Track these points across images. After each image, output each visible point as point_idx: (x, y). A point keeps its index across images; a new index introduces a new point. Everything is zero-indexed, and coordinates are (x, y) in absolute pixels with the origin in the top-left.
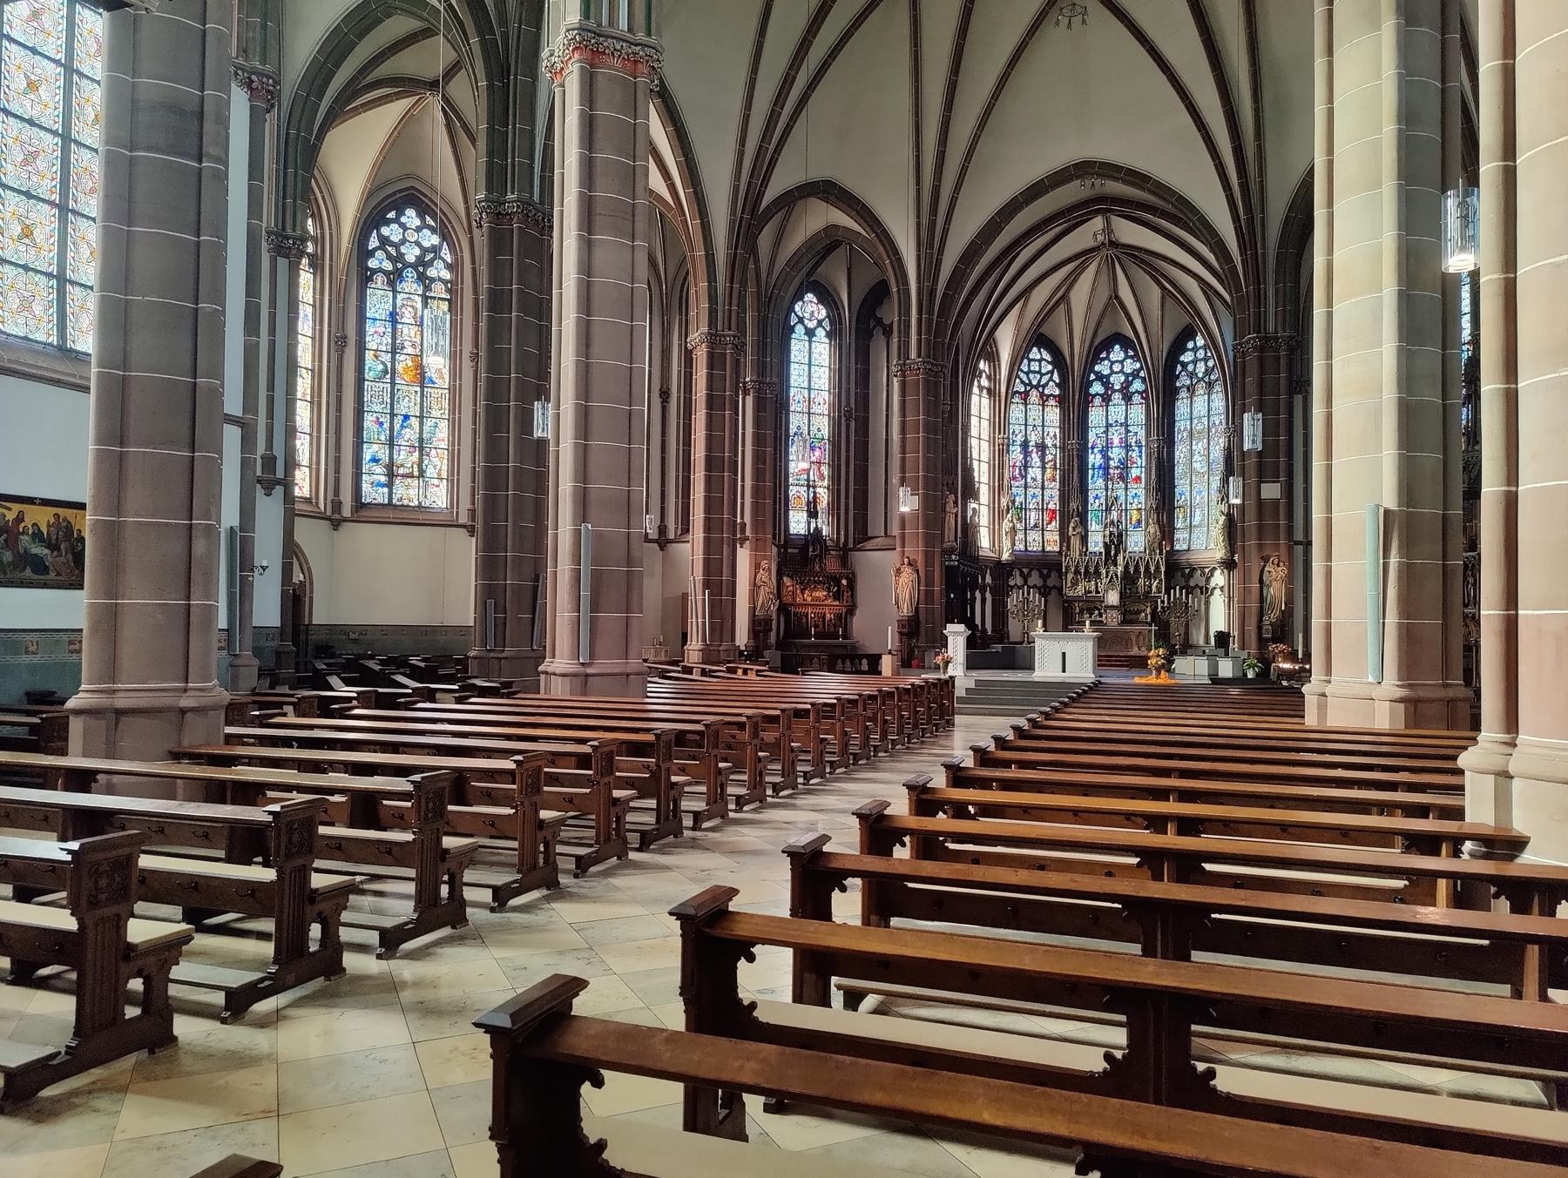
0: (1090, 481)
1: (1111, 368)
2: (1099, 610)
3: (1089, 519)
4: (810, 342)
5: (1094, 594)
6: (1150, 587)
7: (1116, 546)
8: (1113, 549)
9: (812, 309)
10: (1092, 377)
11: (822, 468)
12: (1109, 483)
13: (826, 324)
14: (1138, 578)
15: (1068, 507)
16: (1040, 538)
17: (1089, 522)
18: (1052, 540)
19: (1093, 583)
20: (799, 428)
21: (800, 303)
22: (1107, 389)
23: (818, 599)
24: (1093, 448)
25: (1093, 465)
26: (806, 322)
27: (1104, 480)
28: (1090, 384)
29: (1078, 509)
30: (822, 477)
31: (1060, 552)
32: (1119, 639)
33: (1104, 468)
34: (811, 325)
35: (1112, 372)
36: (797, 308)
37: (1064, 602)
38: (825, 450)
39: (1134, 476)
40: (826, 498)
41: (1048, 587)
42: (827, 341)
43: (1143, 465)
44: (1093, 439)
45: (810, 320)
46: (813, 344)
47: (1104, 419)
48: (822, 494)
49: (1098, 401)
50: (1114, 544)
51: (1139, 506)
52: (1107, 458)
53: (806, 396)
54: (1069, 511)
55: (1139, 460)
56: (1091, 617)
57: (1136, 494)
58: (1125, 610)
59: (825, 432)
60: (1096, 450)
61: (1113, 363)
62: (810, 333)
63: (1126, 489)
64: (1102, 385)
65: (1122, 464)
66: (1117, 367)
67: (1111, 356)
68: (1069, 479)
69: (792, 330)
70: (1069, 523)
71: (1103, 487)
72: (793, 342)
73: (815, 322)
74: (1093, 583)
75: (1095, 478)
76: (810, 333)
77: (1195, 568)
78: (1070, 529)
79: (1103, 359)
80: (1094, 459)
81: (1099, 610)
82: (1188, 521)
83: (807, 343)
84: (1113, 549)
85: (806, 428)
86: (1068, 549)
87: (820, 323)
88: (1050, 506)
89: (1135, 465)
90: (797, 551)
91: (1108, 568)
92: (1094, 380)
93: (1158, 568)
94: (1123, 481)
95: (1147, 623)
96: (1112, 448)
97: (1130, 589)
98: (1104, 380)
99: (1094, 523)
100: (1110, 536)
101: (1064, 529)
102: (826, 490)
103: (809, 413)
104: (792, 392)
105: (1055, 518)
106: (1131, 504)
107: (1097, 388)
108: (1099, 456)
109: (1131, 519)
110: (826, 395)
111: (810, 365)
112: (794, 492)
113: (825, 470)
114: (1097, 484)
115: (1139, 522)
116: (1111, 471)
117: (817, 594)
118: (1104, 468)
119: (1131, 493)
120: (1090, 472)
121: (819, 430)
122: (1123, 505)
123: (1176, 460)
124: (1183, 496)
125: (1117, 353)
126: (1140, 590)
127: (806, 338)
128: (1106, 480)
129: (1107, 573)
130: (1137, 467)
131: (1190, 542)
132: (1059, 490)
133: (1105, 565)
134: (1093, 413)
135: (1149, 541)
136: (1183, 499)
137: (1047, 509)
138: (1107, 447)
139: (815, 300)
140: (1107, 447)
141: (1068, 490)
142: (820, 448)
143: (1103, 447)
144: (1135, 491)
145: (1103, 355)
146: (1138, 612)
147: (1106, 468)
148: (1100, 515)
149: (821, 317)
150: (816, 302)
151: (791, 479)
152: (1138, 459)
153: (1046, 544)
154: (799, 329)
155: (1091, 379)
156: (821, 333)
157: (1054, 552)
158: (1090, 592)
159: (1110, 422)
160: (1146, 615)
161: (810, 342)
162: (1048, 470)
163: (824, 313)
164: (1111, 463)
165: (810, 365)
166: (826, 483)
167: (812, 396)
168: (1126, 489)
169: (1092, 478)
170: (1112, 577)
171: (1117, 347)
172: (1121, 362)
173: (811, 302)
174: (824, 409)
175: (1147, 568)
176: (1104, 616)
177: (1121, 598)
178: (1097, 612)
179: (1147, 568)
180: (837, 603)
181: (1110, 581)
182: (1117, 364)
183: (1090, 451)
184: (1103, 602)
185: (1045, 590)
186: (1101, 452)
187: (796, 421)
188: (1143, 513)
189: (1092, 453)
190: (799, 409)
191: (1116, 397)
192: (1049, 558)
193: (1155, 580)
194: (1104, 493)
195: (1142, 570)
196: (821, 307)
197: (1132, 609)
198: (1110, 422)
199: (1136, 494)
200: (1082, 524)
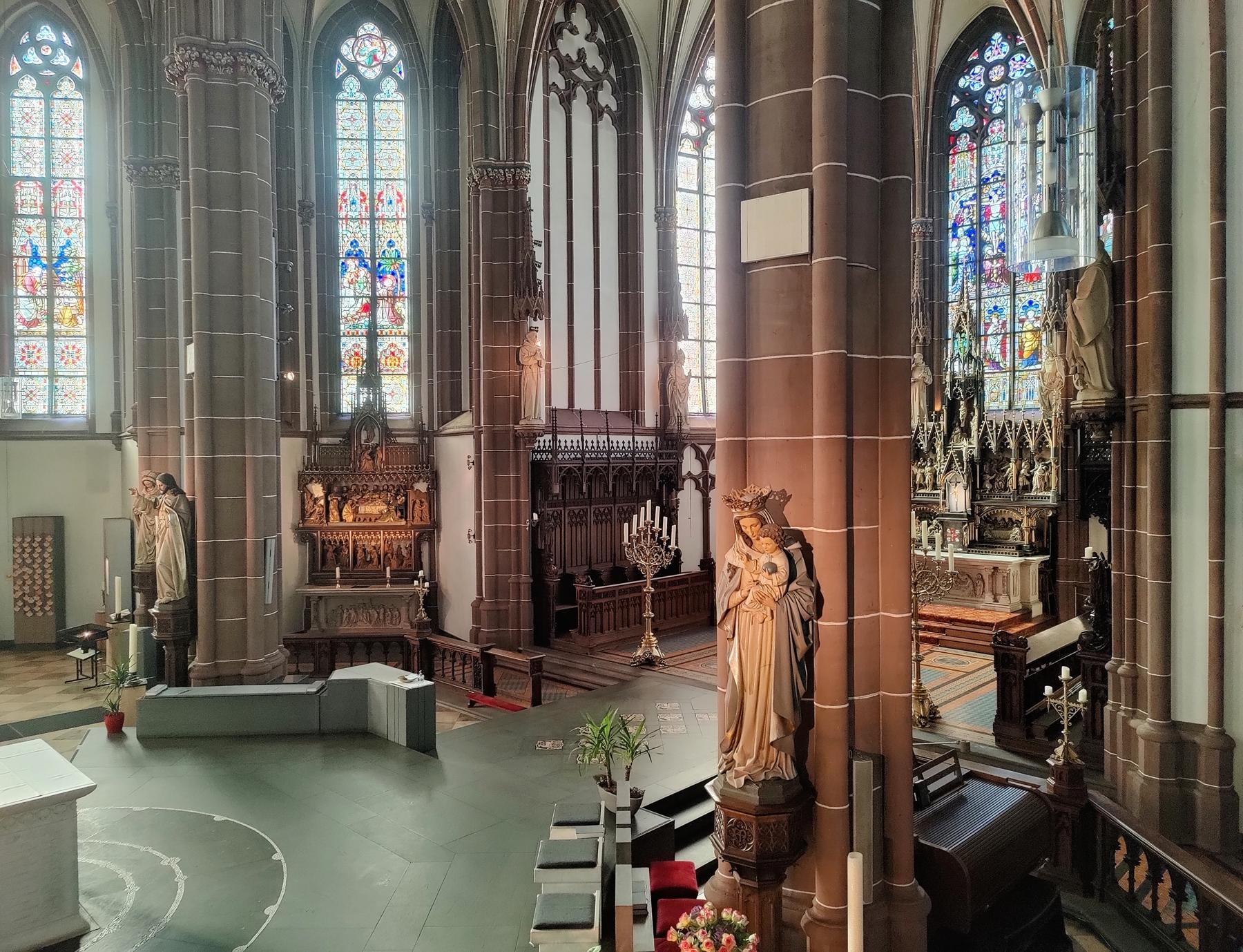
1: (986, 76)
4: (370, 102)
6: (1030, 478)
9: (372, 48)
10: (955, 100)
11: (398, 304)
13: (400, 69)
20: (354, 243)
21: (351, 41)
22: (980, 118)
23: (368, 518)
24: (955, 226)
25: (957, 259)
26: (361, 69)
28: (951, 114)
30: (397, 319)
33: (974, 262)
34: (370, 74)
35: (989, 84)
36: (345, 50)
38: (402, 276)
40: (406, 353)
42: (400, 97)
44: (955, 214)
45: (370, 67)
46: (376, 106)
47: (974, 173)
48: (400, 346)
49: (963, 142)
52: (978, 242)
53: (367, 192)
59: (403, 247)
60: (960, 232)
61: (989, 67)
62: (370, 89)
63: (1014, 294)
64: (971, 112)
66: (997, 74)
67: (987, 54)
69: (337, 86)
72: (339, 107)
73: (378, 70)
76: (370, 89)
79: (974, 64)
80: (959, 247)
83: (364, 106)
85: (368, 244)
87: (388, 70)
90: (337, 440)
92: (957, 106)
93: (1042, 443)
94: (1008, 282)
96: (987, 222)
98: (973, 101)
102: (406, 340)
103: (373, 219)
104: (342, 187)
106: (1022, 321)
107: (964, 119)
108: (965, 241)
109: (1021, 351)
110: (402, 187)
111: (371, 140)
112: (349, 346)
113: (404, 308)
115: (1036, 353)
116: (987, 265)
117: (364, 509)
118: (974, 262)
119: (1023, 299)
120: (952, 271)
121: (391, 244)
122: (1008, 326)
125: (998, 47)
127: (362, 96)
128: (978, 283)
134: (955, 165)
138: (980, 223)
139: (377, 32)
140: (980, 223)
142: (393, 274)
143: (972, 224)
145: (973, 57)
146: (1010, 524)
147: (977, 261)
149: (389, 59)
150: (379, 35)
151: (342, 327)
154: (351, 84)
155: (953, 104)
156: (389, 85)
158: (922, 486)
159: (985, 174)
161: (370, 102)
163: (393, 51)
164: (988, 251)
165: (371, 140)
166: (406, 328)
167: (377, 191)
168: (1014, 294)
169: (954, 281)
171: (997, 36)
172: (1005, 62)
173: (370, 36)
174: (401, 210)
175: (1022, 443)
179: (1022, 443)
180: (403, 523)
182: (996, 69)
183: (950, 235)
186: (969, 233)
187: (350, 233)
189: (954, 236)
190: (354, 215)
191: (996, 129)
195: (1012, 445)
196: (388, 43)
198: (985, 174)
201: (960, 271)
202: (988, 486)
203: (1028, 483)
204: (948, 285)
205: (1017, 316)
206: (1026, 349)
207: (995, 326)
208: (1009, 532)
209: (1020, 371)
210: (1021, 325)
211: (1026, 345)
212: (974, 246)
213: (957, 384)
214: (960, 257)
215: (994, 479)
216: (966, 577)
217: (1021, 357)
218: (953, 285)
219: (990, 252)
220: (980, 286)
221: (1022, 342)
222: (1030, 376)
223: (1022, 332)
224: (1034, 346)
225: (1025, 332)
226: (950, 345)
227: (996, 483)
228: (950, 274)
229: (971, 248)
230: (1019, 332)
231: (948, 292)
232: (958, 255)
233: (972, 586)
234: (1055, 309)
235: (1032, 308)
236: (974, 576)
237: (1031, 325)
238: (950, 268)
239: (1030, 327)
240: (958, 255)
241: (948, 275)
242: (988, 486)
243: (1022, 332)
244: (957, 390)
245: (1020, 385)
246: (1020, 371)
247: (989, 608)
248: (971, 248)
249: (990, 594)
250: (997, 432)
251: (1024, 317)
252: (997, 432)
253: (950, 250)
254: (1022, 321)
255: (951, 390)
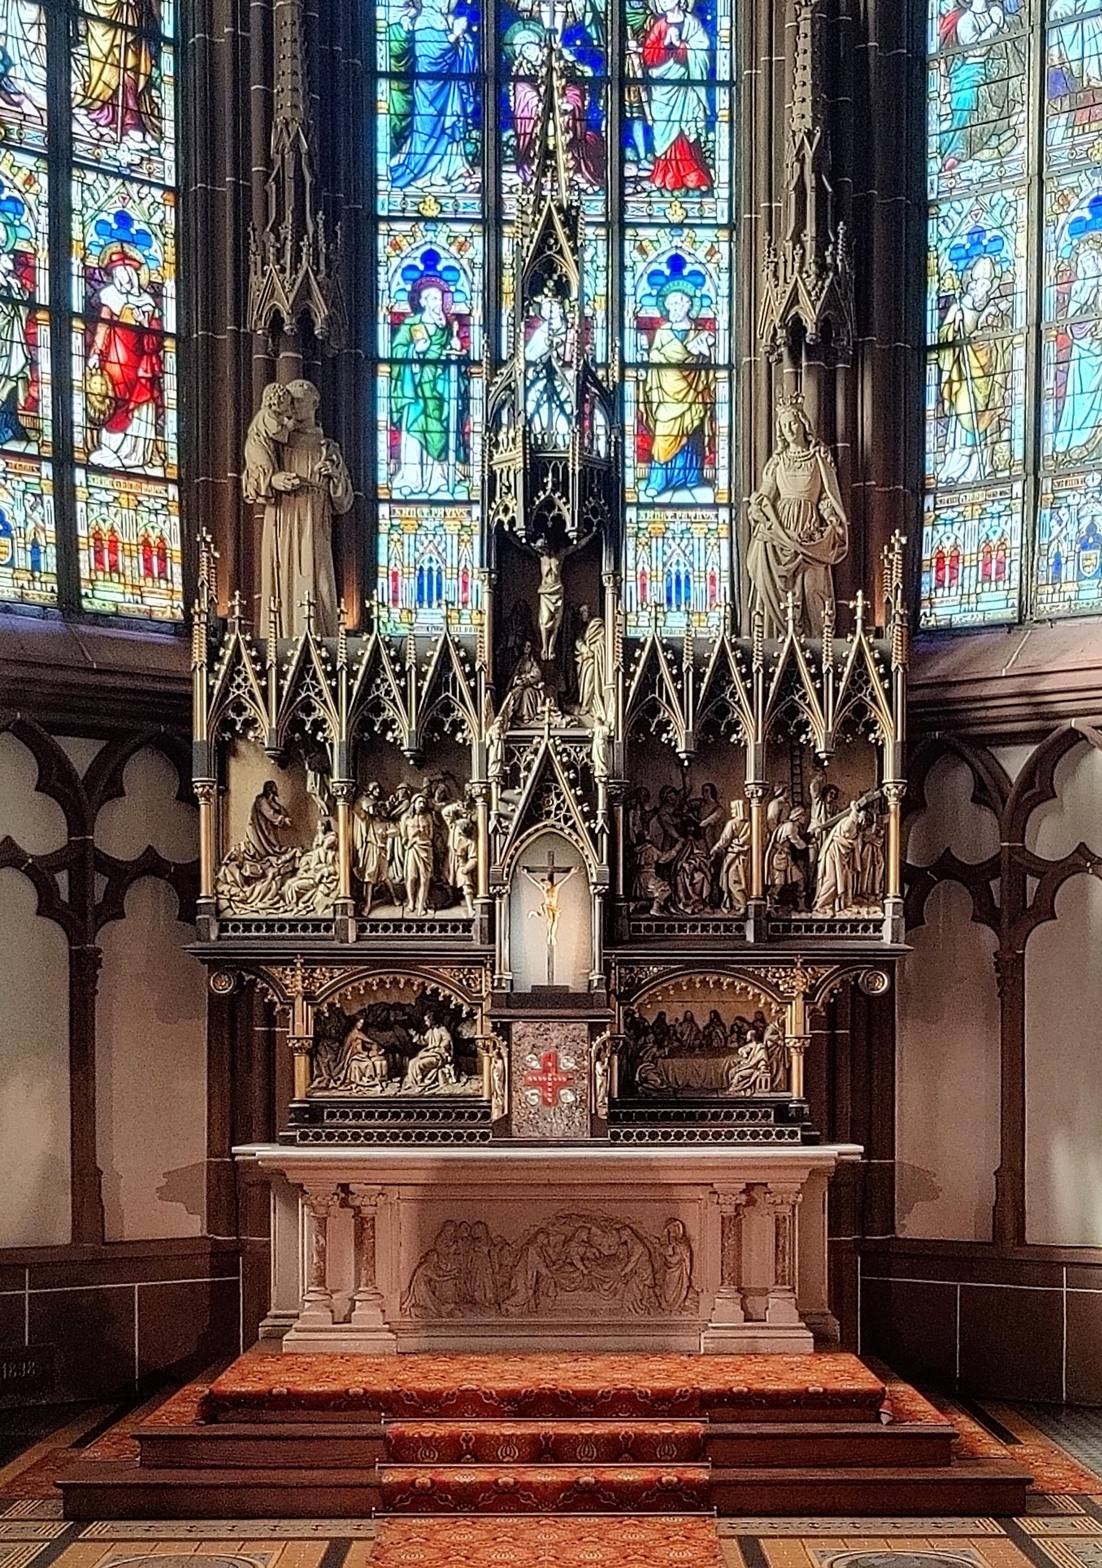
0: (383, 163)
2: (450, 1018)
3: (382, 416)
5: (416, 909)
7: (564, 575)
8: (549, 584)
12: (511, 178)
14: (715, 798)
15: (240, 314)
16: (45, 513)
17: (383, 439)
18: (128, 538)
19: (411, 824)
25: (408, 54)
27: (476, 160)
29: (305, 319)
31: (183, 629)
32: (607, 1243)
37: (217, 963)
39: (661, 146)
41: (106, 864)
43: (723, 74)
50: (557, 540)
51: (698, 345)
54: (243, 342)
55: (698, 39)
56: (396, 1071)
57: (676, 263)
58: (635, 1026)
65: (589, 55)
68: (241, 110)
70: (245, 413)
71: (471, 204)
74: (411, 824)
75: (418, 144)
77: (1074, 736)
78: (255, 454)
81: (450, 1018)
82: (1019, 429)
84: (549, 584)
86: (250, 611)
88: (111, 298)
89: (671, 70)
91: (516, 720)
94: (598, 176)
95: (782, 1112)
97: (666, 872)
99: (410, 445)
100: (533, 482)
101: (212, 465)
105: (155, 383)
106: (647, 326)
114: (434, 181)
118: (476, 79)
122: (599, 337)
123: (935, 31)
124: (983, 269)
126: (731, 879)
129: (511, 749)
130: (685, 83)
131: (1028, 571)
132: (179, 193)
133: (500, 688)
135: (774, 552)
136: (979, 290)
137: (93, 312)
141: (242, 196)
144: (666, 244)
148: (450, 389)
152: (691, 22)
153: (85, 560)
157: (149, 621)
160: (778, 1056)
162: (100, 39)
169: (400, 138)
170: (545, 780)
176: (492, 1067)
177: (610, 936)
178: (437, 1037)
181: (533, 813)
184: (485, 961)
185: (80, 886)
188: (722, 391)
192: (111, 657)
193: (835, 810)
194: (477, 249)
197: (674, 1014)
199: (676, 263)
200: (332, 433)
201: (423, 107)
202: (655, 888)
203: (796, 875)
204: (373, 152)
205: (629, 307)
206: (661, 429)
207: (553, 333)
208: (725, 1062)
209: (640, 506)
210: (644, 340)
211: (663, 414)
212: (474, 17)
213: (549, 479)
214: (420, 49)
215: (676, 860)
216: (626, 1234)
217: (645, 454)
218: (395, 150)
219: (534, 54)
220: (498, 172)
221: (648, 402)
222: (677, 527)
223: (647, 366)
224: (691, 421)
225: (659, 366)
226: (382, 383)
227: (682, 880)
228: (382, 107)
229: (461, 23)
230: (637, 366)
231: (374, 177)
232: (411, 38)
233: (647, 1274)
234: (822, 268)
235: (683, 285)
236: (651, 1227)
237: (677, 346)
238: (383, 85)
239: (674, 352)
240: (411, 38)
241: (374, 112)
242: (655, 888)
243: (647, 366)
244: (549, 504)
245: (643, 553)
246: (640, 506)
247: (733, 1346)
248: (461, 23)
249: (728, 1291)
250: (698, 677)
251: (655, 313)
252: (698, 677)
253: (380, 12)
254: (647, 326)
255: (528, 502)
